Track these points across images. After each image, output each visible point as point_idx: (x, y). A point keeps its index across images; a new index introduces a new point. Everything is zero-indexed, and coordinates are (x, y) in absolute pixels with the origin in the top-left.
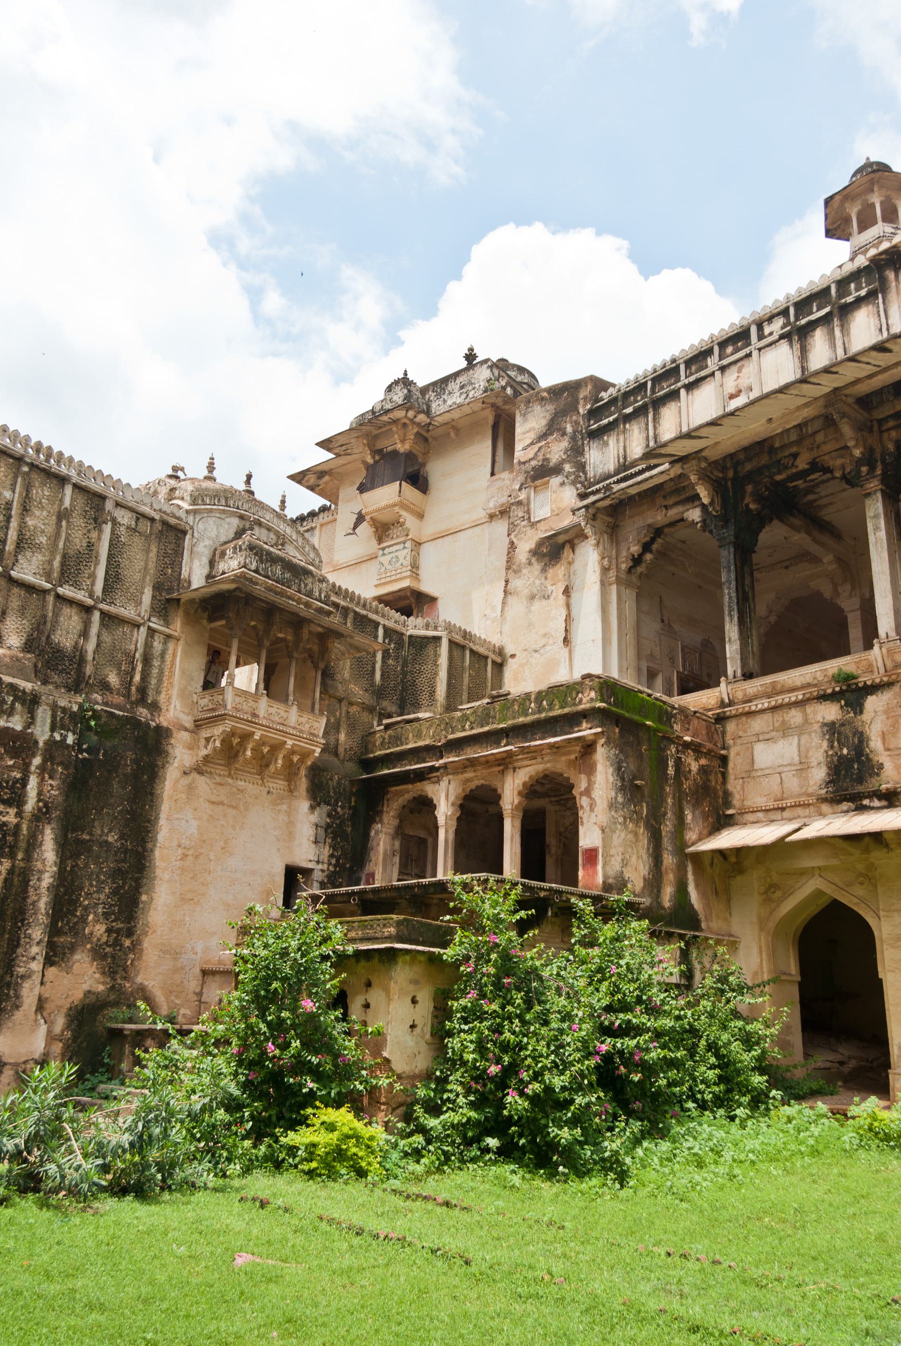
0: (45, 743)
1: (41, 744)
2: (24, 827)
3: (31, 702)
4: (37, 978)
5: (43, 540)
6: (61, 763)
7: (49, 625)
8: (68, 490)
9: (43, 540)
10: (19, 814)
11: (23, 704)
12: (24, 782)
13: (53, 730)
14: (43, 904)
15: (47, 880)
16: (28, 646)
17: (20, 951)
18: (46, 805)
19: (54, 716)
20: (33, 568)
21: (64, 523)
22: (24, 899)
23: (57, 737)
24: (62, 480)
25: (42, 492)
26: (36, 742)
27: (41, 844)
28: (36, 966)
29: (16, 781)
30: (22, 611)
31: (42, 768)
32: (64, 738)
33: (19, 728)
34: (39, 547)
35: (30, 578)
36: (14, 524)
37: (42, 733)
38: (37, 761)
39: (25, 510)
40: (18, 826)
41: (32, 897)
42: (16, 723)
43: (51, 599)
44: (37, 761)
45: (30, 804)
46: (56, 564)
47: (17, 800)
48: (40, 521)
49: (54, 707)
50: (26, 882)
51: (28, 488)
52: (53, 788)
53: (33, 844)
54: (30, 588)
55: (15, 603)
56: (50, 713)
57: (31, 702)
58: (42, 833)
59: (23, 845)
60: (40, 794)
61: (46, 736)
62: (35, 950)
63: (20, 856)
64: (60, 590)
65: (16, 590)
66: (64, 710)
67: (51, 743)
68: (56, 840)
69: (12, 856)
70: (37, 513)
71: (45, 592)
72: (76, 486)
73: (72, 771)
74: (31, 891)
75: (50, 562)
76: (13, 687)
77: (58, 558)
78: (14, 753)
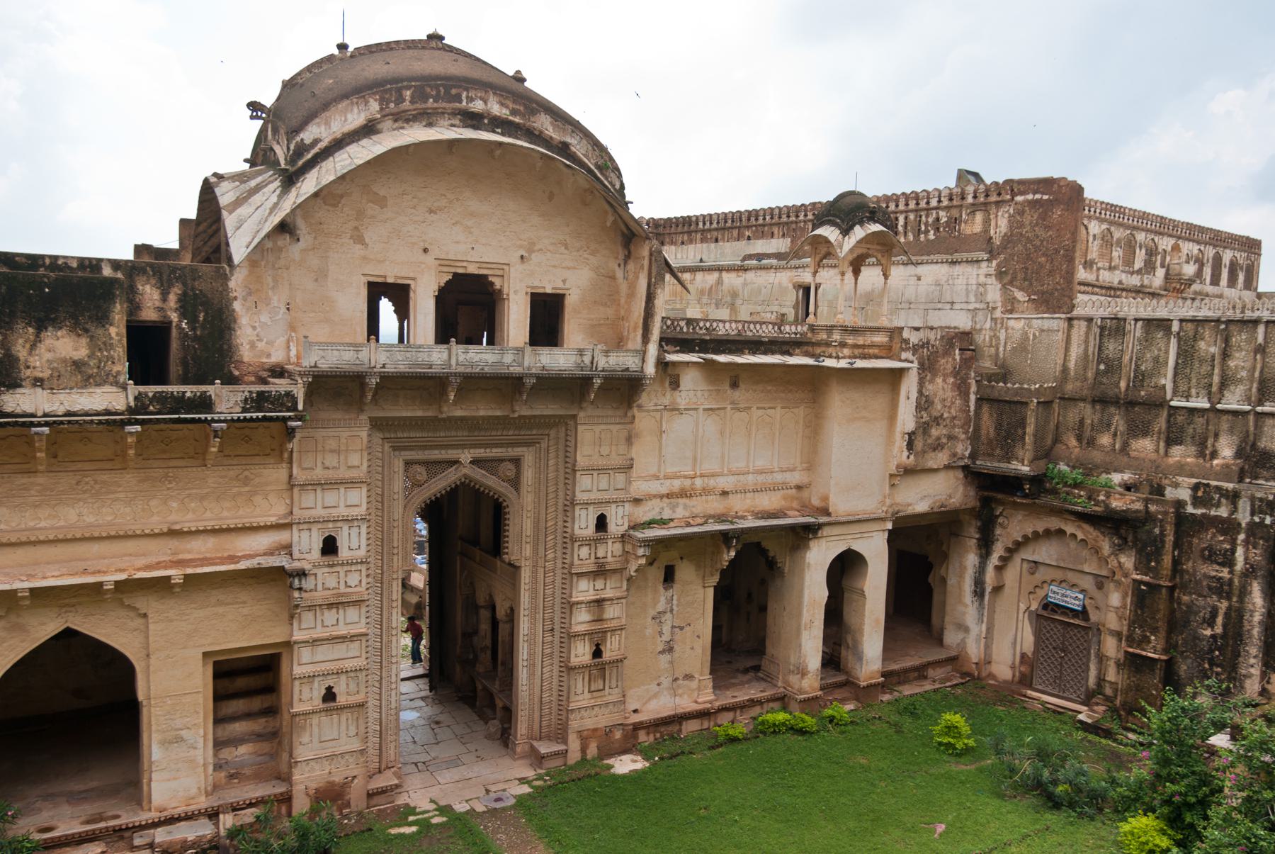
0: (1248, 524)
1: (1244, 525)
2: (1236, 581)
3: (1234, 497)
4: (1256, 679)
5: (1244, 374)
6: (1261, 538)
7: (1251, 438)
8: (1261, 329)
9: (1244, 374)
10: (1231, 572)
11: (1227, 498)
12: (1233, 551)
13: (1253, 514)
14: (1256, 632)
15: (1257, 617)
16: (1239, 454)
17: (1241, 659)
18: (1252, 566)
19: (1253, 506)
20: (1237, 397)
21: (1258, 357)
22: (1241, 627)
23: (1257, 519)
24: (1256, 322)
25: (1239, 338)
26: (1239, 524)
27: (1250, 593)
28: (1255, 671)
29: (1227, 550)
30: (1231, 431)
31: (1246, 542)
32: (1263, 520)
33: (1225, 515)
34: (1241, 380)
35: (1234, 407)
36: (1216, 371)
37: (1244, 516)
38: (1242, 537)
39: (1225, 355)
40: (1231, 580)
41: (1247, 626)
42: (1223, 512)
43: (1251, 417)
44: (1242, 537)
45: (1240, 565)
46: (1254, 390)
47: (1229, 562)
48: (1240, 361)
49: (1252, 499)
50: (1241, 617)
51: (1227, 341)
52: (1257, 555)
53: (1244, 592)
54: (1235, 413)
55: (1225, 426)
56: (1248, 504)
57: (1234, 497)
58: (1251, 585)
59: (1237, 592)
60: (1246, 559)
61: (1248, 519)
62: (1252, 661)
63: (1235, 599)
64: (1259, 409)
65: (1225, 418)
66: (1261, 500)
67: (1252, 525)
68: (1263, 591)
69: (1229, 598)
70: (1237, 355)
71: (1248, 413)
72: (1268, 322)
73: (1271, 543)
74: (1246, 623)
75: (1250, 389)
76: (1217, 487)
77: (1255, 385)
78: (1224, 532)
